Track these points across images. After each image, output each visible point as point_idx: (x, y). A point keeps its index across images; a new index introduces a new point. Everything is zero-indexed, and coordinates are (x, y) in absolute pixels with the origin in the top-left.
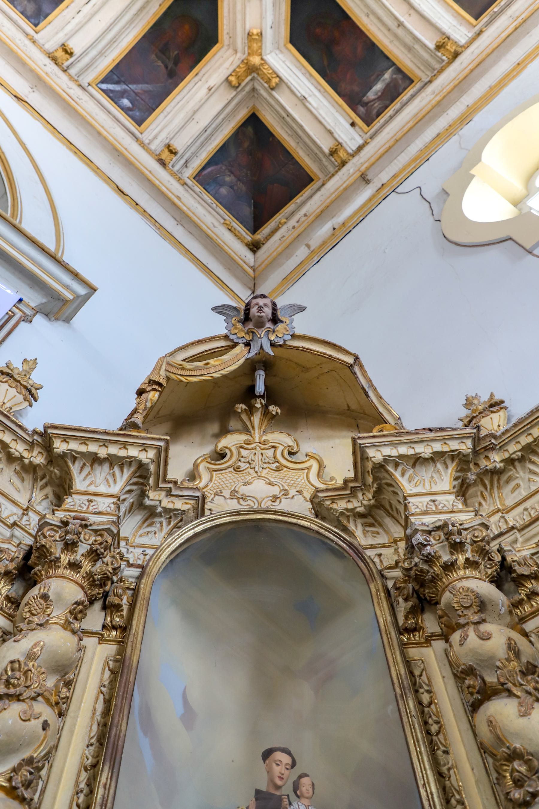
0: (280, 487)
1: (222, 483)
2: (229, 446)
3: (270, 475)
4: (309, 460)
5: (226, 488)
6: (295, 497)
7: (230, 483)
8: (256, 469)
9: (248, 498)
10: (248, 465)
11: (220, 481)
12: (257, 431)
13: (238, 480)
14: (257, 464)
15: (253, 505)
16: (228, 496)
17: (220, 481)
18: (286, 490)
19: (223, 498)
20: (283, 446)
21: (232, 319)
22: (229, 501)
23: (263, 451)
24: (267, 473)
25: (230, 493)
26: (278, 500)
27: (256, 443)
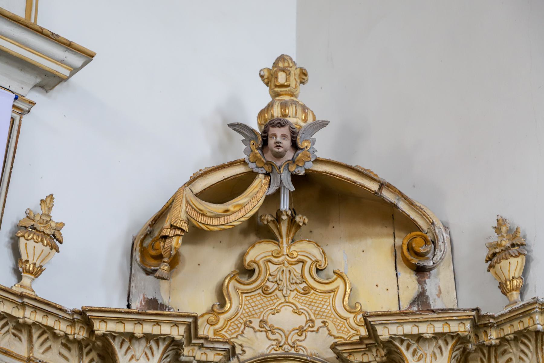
0: (306, 317)
1: (251, 309)
2: (257, 259)
3: (297, 299)
4: (336, 279)
5: (255, 316)
6: (320, 330)
7: (259, 309)
8: (284, 292)
9: (276, 331)
10: (276, 285)
11: (249, 306)
12: (285, 240)
13: (267, 306)
14: (285, 283)
15: (280, 339)
16: (257, 328)
17: (249, 306)
18: (312, 321)
19: (252, 329)
20: (311, 259)
21: (250, 141)
22: (258, 334)
23: (291, 267)
24: (295, 297)
25: (259, 323)
26: (304, 333)
27: (284, 255)
